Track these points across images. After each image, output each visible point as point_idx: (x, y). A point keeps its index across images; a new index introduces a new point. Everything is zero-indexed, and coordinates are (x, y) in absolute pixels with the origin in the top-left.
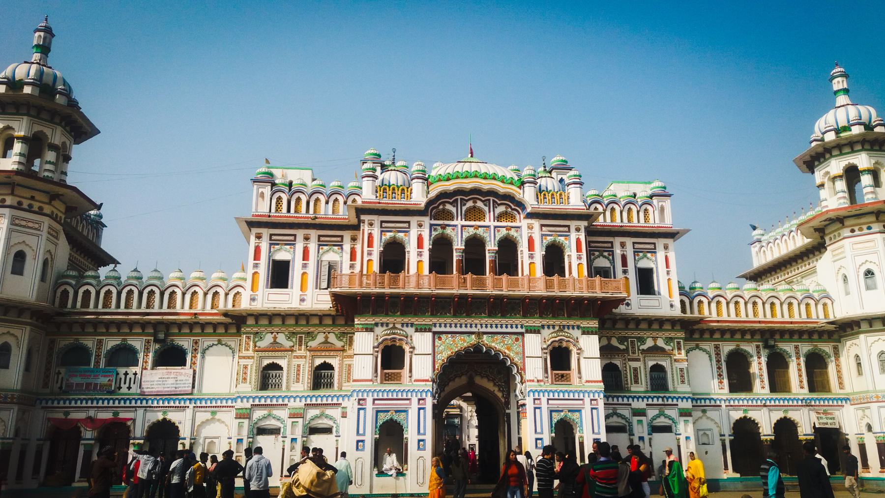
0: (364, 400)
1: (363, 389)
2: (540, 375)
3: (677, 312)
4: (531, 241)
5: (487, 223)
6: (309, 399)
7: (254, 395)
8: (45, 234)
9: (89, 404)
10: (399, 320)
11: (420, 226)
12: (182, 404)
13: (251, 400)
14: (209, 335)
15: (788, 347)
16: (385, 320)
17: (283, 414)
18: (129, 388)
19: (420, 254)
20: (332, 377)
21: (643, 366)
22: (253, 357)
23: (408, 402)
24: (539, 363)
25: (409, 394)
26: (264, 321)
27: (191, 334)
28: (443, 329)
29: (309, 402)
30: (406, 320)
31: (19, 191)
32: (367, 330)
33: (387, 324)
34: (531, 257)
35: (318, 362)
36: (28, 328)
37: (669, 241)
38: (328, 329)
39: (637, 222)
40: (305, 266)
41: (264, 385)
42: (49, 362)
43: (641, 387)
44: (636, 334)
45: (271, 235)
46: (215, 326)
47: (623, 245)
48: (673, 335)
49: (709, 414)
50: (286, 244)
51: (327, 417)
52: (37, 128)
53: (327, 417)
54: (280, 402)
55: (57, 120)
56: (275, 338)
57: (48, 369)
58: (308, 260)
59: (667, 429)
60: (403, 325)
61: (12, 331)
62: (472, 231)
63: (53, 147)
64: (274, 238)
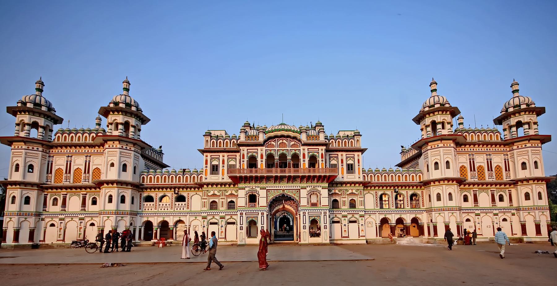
2: (306, 204)
3: (361, 180)
4: (304, 155)
5: (287, 148)
15: (404, 192)
20: (234, 205)
21: (347, 200)
24: (306, 199)
34: (304, 161)
35: (229, 200)
37: (360, 153)
39: (348, 146)
40: (223, 167)
41: (211, 208)
43: (347, 207)
44: (345, 188)
47: (342, 155)
48: (359, 188)
49: (371, 216)
59: (355, 222)
62: (281, 152)
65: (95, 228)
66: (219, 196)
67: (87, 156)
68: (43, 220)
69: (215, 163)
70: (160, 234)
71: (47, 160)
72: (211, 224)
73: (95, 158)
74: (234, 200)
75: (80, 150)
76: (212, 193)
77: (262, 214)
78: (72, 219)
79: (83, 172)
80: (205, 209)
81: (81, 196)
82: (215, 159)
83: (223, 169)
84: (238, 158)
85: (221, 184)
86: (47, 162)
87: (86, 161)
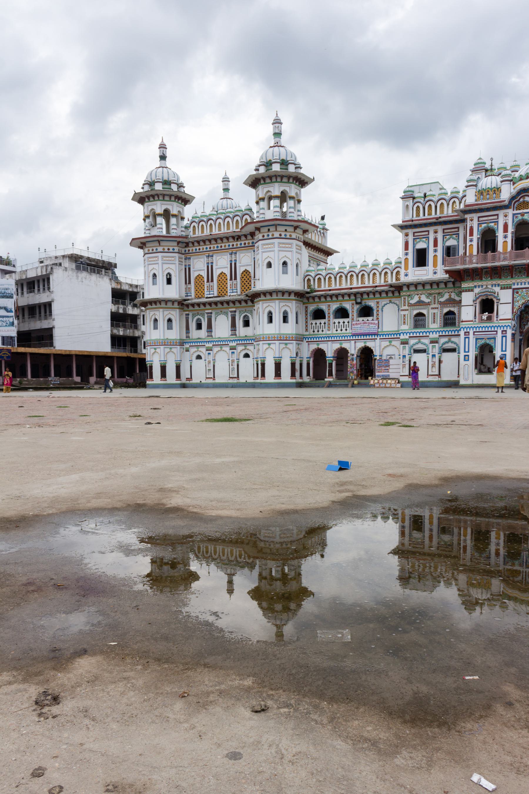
0: (468, 332)
1: (467, 326)
6: (441, 333)
7: (410, 331)
8: (294, 249)
9: (328, 339)
10: (490, 283)
11: (506, 216)
12: (373, 337)
13: (408, 334)
14: (384, 298)
16: (480, 283)
17: (426, 341)
18: (346, 330)
19: (505, 237)
20: (455, 319)
22: (408, 310)
23: (495, 333)
25: (496, 328)
26: (412, 288)
27: (375, 298)
28: (519, 286)
29: (441, 334)
30: (494, 282)
31: (279, 228)
32: (469, 291)
33: (482, 286)
35: (446, 310)
36: (294, 302)
38: (451, 290)
40: (435, 251)
41: (416, 326)
42: (307, 318)
45: (414, 233)
46: (387, 293)
50: (423, 238)
51: (452, 342)
52: (282, 189)
53: (452, 342)
54: (424, 334)
55: (291, 180)
56: (420, 298)
57: (307, 322)
58: (437, 246)
60: (492, 286)
61: (287, 304)
63: (292, 198)
64: (416, 234)
65: (249, 360)
66: (429, 304)
67: (231, 254)
68: (187, 350)
69: (421, 245)
70: (337, 371)
71: (184, 264)
72: (417, 351)
73: (242, 255)
74: (455, 310)
75: (223, 245)
76: (416, 299)
77: (504, 332)
78: (221, 348)
79: (229, 278)
80: (405, 327)
81: (230, 314)
82: (420, 238)
83: (435, 255)
84: (461, 233)
85: (432, 283)
86: (184, 268)
87: (231, 261)
